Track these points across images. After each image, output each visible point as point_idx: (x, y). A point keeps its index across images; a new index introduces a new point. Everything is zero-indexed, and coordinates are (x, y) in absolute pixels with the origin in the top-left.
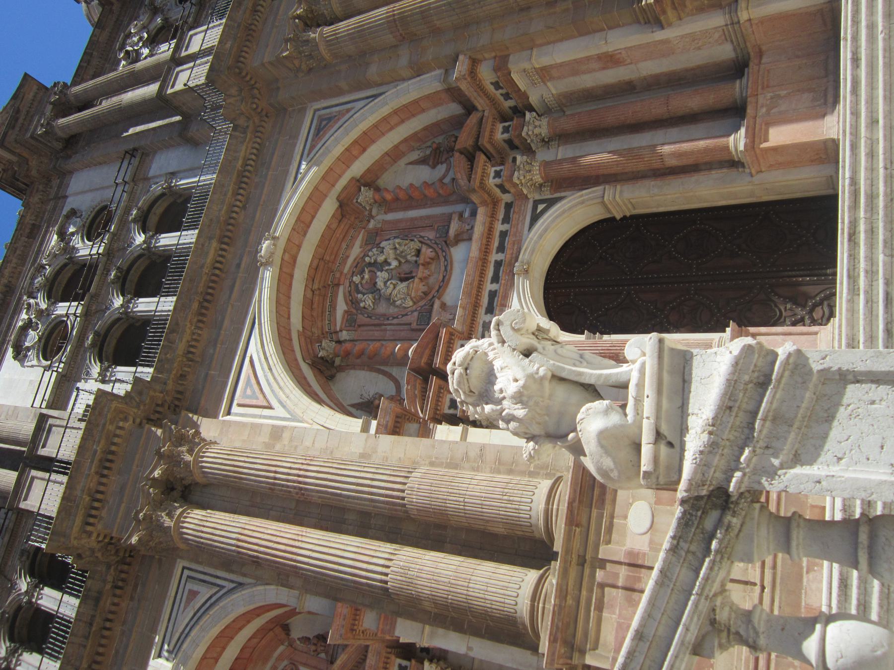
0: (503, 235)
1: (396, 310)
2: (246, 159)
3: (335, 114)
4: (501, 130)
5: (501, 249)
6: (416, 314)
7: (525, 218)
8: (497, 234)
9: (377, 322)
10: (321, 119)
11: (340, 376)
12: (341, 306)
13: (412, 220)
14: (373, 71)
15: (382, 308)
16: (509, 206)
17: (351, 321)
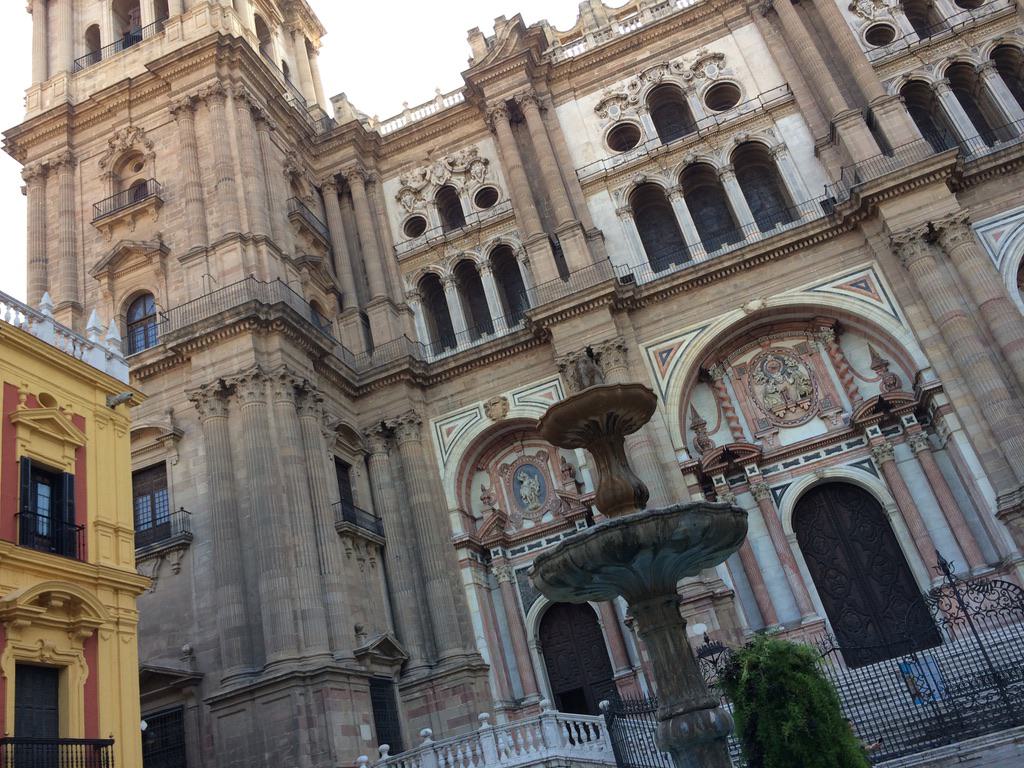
0: (839, 449)
1: (761, 401)
2: (812, 237)
3: (872, 289)
4: (908, 416)
5: (828, 452)
6: (764, 416)
7: (856, 458)
8: (838, 445)
9: (748, 390)
10: (864, 281)
11: (705, 385)
12: (747, 358)
13: (827, 374)
14: (912, 311)
15: (759, 389)
16: (860, 442)
17: (741, 369)
